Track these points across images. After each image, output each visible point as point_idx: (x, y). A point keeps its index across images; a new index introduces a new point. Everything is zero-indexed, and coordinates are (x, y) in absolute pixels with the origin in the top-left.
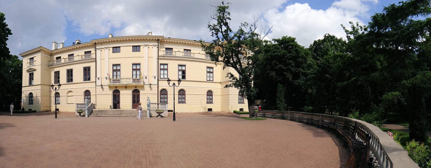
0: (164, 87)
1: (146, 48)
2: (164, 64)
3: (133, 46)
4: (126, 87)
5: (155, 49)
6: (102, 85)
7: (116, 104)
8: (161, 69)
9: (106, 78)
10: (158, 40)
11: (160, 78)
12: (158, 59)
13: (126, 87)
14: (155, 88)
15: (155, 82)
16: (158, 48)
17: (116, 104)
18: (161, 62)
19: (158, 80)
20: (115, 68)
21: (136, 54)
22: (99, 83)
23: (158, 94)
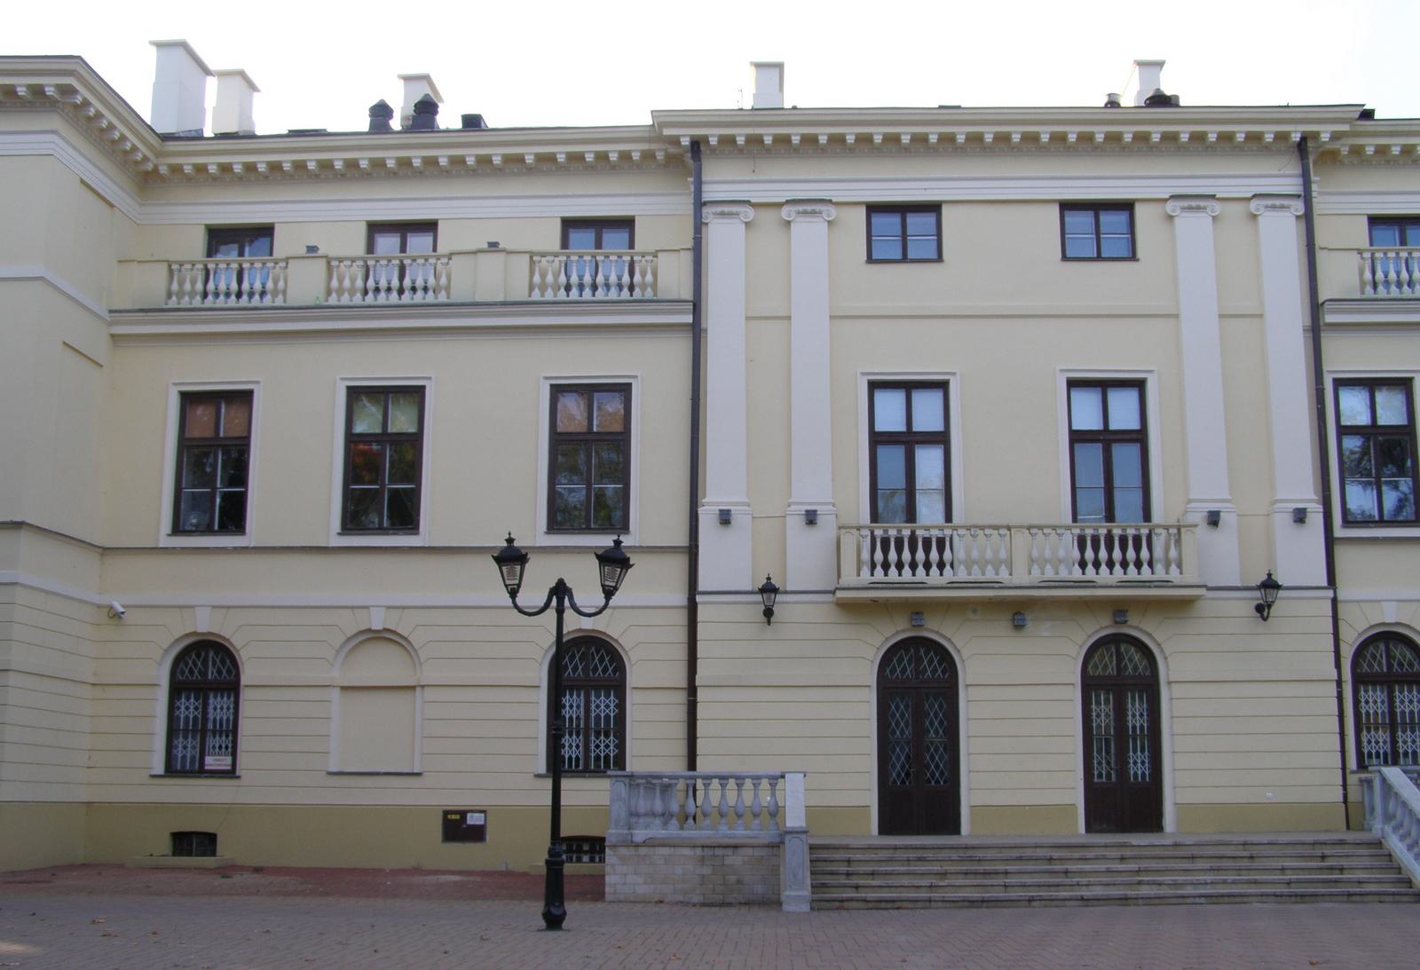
0: (1389, 615)
1: (1194, 228)
2: (1371, 385)
3: (1066, 206)
4: (1017, 611)
5: (1280, 232)
6: (769, 589)
7: (919, 787)
8: (1343, 431)
9: (811, 518)
10: (1302, 147)
11: (1348, 521)
12: (1315, 330)
13: (1017, 611)
14: (1303, 619)
15: (1300, 558)
16: (1308, 218)
17: (919, 787)
18: (1345, 357)
19: (1330, 542)
20: (890, 413)
21: (1102, 283)
22: (727, 563)
23: (1339, 683)
